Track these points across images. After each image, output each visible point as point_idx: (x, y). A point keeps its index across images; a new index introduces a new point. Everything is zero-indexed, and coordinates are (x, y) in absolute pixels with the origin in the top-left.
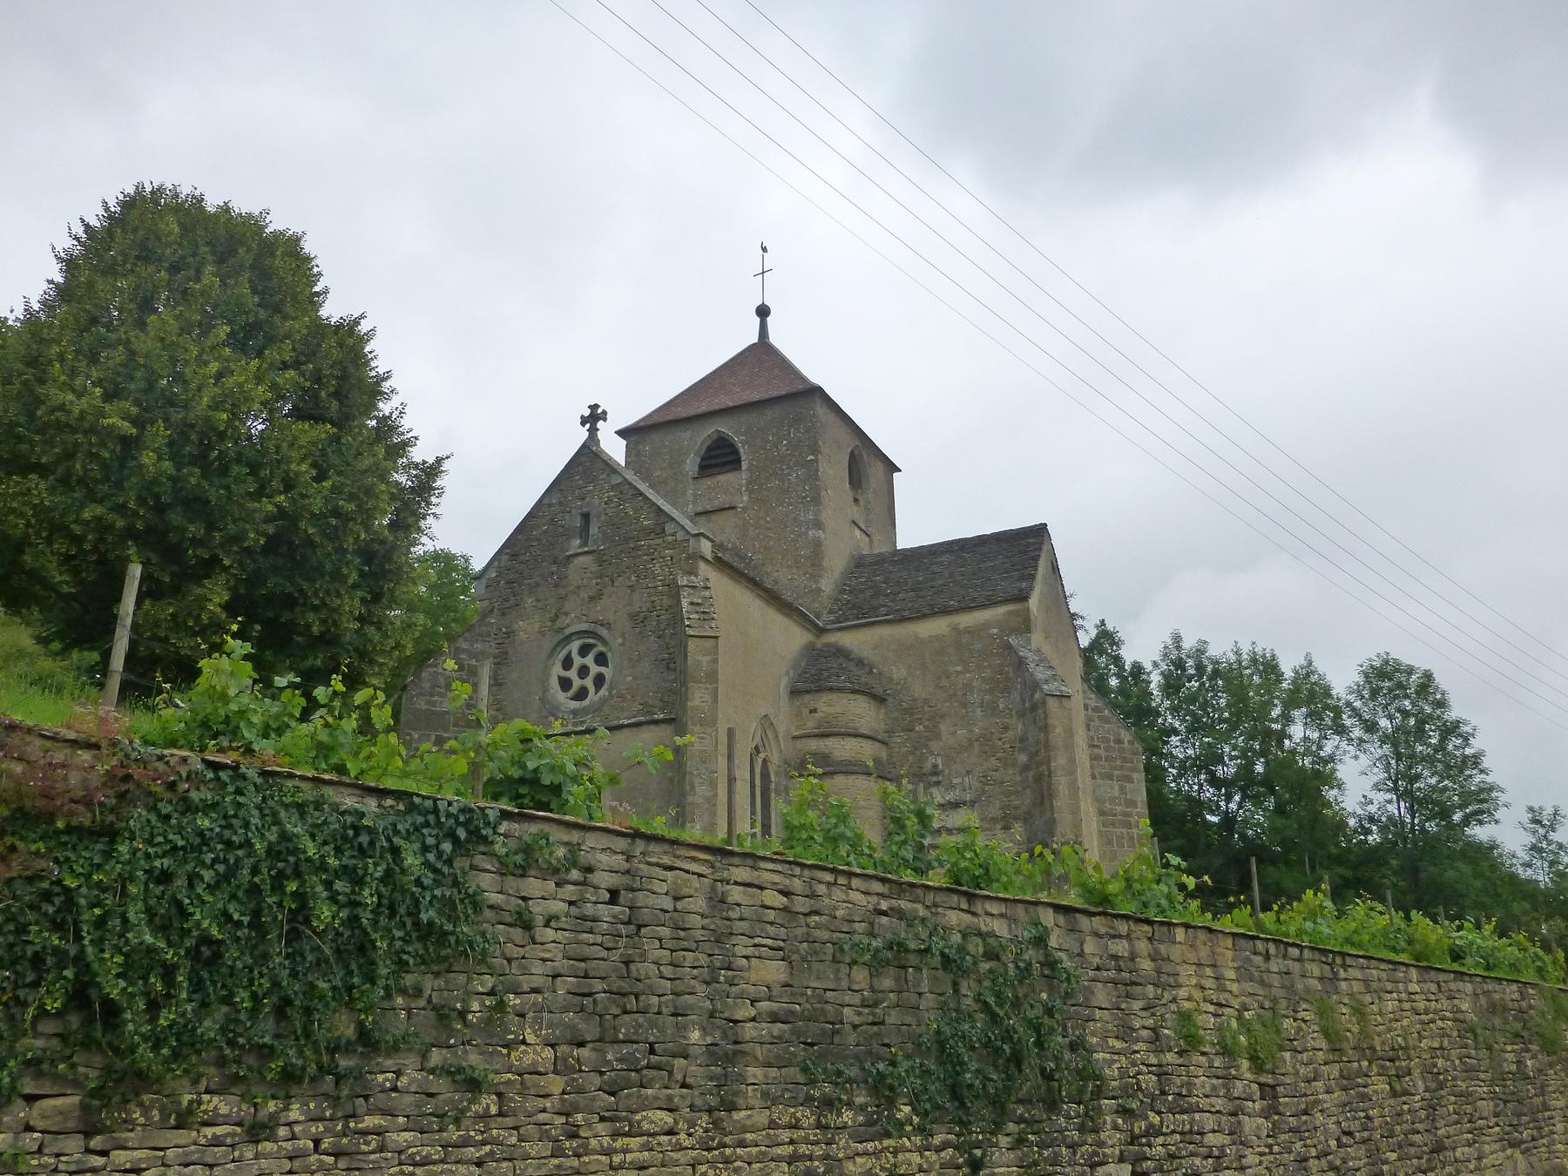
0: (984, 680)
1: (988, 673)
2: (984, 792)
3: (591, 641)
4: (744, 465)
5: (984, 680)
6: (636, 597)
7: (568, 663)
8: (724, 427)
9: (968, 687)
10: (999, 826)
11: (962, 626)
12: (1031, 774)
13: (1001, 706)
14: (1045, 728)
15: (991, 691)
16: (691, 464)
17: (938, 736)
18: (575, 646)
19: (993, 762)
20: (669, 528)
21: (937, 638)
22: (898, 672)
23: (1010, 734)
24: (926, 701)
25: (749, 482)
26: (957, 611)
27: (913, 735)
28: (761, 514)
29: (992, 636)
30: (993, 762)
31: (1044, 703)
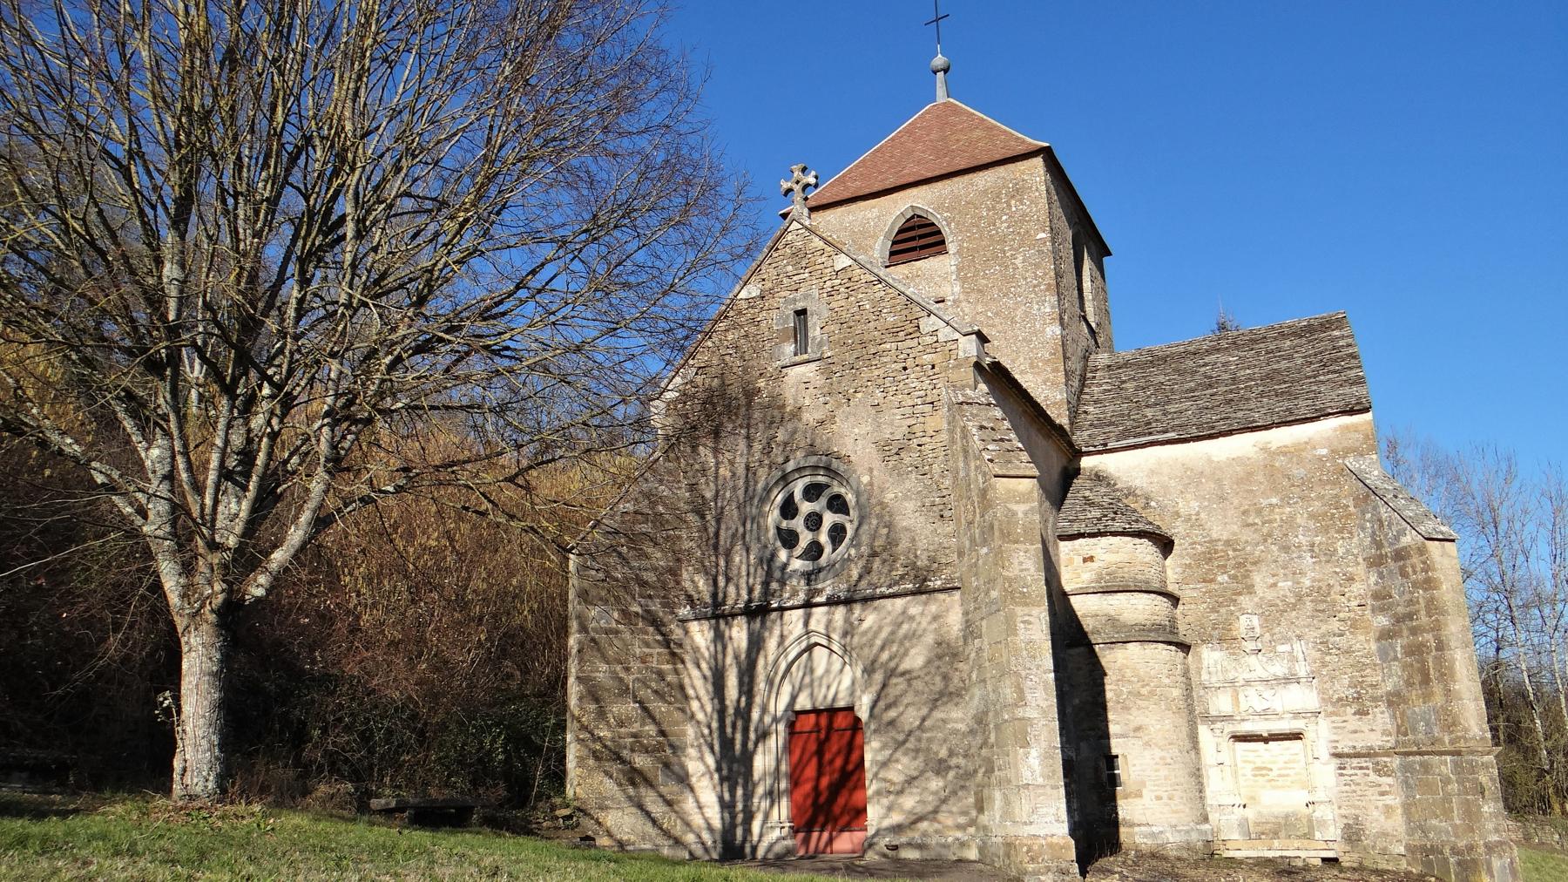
0: (1312, 516)
1: (1316, 506)
3: (821, 479)
4: (952, 247)
5: (1312, 516)
6: (885, 417)
7: (789, 509)
9: (1290, 522)
10: (1350, 710)
12: (1399, 644)
13: (1341, 551)
14: (1429, 584)
16: (879, 248)
17: (1250, 589)
18: (798, 488)
19: (1335, 625)
20: (927, 324)
21: (1239, 461)
23: (1357, 588)
24: (1228, 543)
25: (959, 270)
29: (1320, 459)
30: (1335, 625)
31: (1422, 551)
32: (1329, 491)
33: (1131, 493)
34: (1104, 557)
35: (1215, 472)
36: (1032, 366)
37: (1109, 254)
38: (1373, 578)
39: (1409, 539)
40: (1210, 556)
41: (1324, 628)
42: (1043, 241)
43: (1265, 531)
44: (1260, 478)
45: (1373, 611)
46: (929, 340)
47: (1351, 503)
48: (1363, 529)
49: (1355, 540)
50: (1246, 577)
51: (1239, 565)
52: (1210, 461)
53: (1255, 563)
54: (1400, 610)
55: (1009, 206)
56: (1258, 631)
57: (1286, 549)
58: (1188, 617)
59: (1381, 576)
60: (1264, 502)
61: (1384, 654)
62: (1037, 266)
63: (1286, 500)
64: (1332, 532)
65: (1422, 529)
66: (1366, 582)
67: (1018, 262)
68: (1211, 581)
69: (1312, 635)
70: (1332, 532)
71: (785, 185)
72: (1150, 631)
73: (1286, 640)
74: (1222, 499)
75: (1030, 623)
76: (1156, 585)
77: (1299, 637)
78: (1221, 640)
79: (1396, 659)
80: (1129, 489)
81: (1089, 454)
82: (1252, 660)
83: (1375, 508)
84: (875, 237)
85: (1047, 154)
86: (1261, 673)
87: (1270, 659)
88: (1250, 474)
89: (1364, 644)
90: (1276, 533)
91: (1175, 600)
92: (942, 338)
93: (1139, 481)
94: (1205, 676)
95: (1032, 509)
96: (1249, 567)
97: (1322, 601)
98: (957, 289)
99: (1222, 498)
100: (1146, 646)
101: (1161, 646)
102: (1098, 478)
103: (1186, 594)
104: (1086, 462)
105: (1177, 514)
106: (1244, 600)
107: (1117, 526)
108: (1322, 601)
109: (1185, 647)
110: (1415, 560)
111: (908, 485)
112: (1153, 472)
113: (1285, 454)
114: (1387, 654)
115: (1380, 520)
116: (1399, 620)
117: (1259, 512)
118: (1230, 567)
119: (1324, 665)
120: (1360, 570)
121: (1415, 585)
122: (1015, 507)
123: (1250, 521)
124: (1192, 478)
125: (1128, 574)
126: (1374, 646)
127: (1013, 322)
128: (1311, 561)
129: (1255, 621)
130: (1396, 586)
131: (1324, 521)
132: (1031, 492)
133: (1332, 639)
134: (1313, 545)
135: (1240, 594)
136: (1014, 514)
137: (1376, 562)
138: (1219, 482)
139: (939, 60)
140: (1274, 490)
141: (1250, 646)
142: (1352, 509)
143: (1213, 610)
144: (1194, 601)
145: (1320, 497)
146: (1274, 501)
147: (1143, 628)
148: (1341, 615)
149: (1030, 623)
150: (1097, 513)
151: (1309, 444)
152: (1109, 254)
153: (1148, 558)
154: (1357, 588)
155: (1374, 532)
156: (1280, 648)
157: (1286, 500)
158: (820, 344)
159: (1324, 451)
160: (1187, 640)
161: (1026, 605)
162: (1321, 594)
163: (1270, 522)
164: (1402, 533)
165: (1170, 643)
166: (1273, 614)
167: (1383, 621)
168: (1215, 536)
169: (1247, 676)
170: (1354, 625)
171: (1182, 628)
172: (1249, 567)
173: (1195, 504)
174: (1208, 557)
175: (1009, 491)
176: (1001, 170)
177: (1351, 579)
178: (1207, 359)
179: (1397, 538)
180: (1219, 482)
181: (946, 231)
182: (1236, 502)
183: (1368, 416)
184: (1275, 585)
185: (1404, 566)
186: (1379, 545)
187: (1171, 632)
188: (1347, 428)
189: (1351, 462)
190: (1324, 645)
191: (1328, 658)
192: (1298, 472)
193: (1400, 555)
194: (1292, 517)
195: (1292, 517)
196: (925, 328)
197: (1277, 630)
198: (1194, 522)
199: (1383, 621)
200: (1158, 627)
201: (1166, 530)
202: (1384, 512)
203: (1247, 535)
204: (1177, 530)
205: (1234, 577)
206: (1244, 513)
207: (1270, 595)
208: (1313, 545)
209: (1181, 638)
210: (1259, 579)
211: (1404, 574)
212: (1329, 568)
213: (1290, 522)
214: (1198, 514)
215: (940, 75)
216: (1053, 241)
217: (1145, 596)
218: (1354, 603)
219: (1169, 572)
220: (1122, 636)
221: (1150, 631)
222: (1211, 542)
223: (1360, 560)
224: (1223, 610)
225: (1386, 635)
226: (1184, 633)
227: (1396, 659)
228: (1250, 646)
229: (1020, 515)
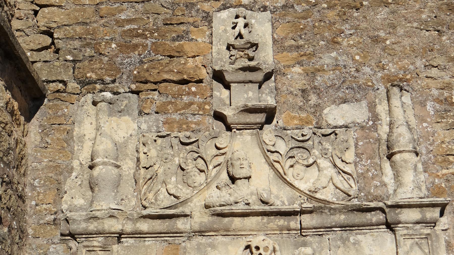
73: (352, 89)
77: (398, 84)
78: (143, 84)
82: (242, 146)
86: (260, 183)
87: (302, 145)
94: (75, 199)
129: (262, 29)
156: (335, 115)
169: (214, 196)
197: (327, 59)
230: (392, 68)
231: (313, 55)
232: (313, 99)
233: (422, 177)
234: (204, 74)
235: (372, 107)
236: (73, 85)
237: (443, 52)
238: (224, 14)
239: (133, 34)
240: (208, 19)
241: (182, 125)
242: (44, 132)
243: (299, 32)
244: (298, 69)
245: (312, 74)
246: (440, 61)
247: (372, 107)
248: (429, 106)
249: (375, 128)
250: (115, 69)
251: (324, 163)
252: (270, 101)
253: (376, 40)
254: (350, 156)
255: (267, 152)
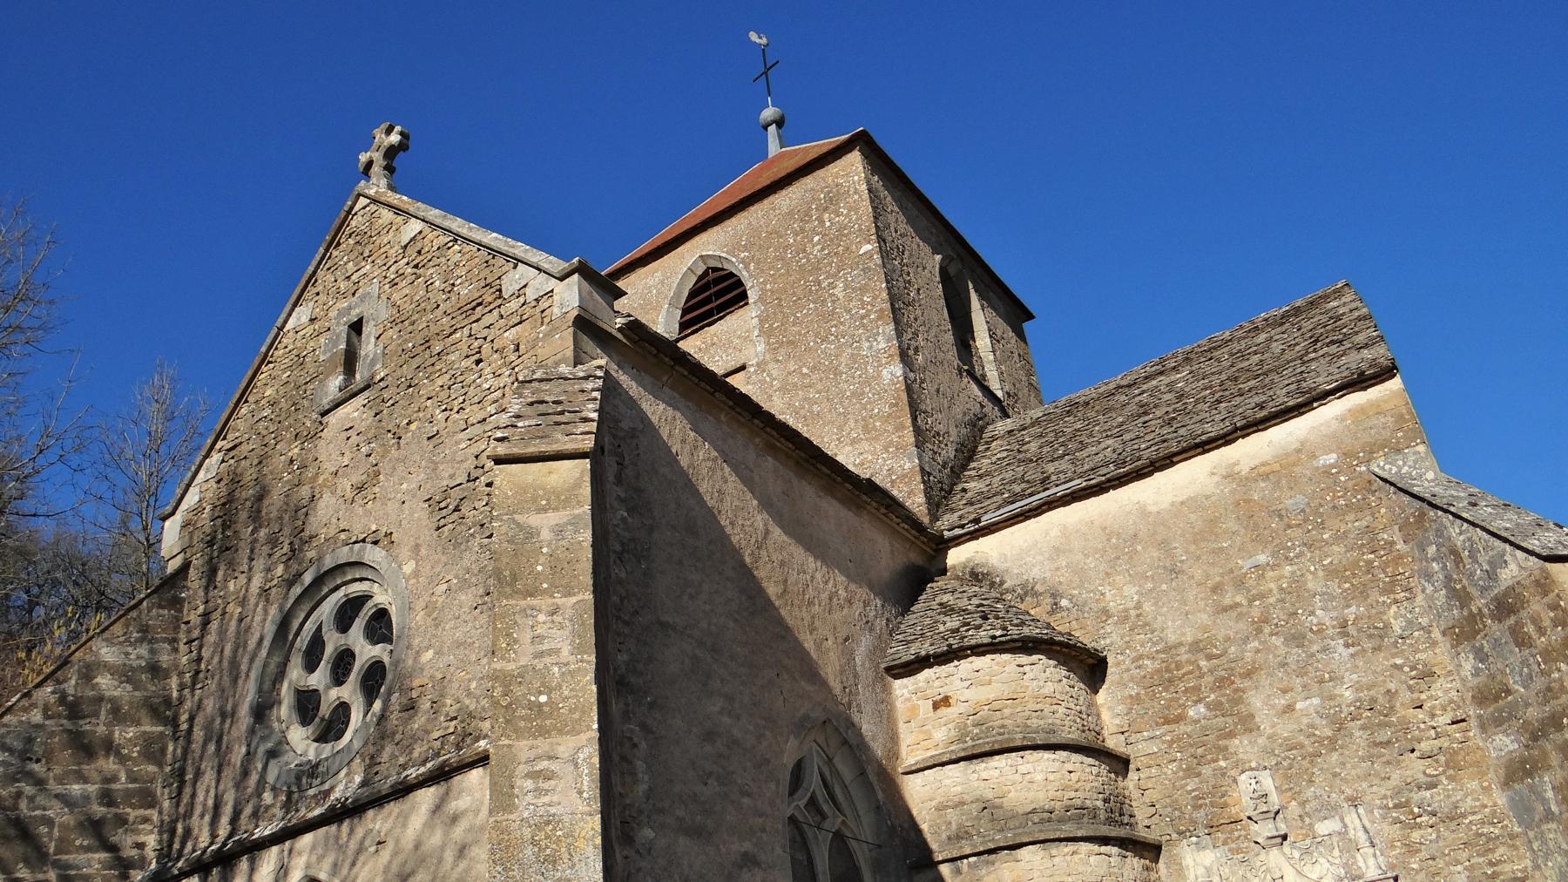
0: (1332, 573)
2: (1411, 849)
4: (752, 295)
5: (1332, 573)
8: (710, 245)
9: (1296, 590)
11: (1244, 469)
12: (1547, 783)
13: (1397, 626)
15: (1362, 593)
17: (1248, 724)
19: (1415, 768)
21: (1192, 503)
22: (1121, 594)
23: (1442, 690)
24: (1196, 647)
26: (1226, 439)
27: (1183, 728)
28: (792, 366)
29: (1326, 472)
30: (1415, 768)
31: (1544, 585)
32: (1355, 524)
33: (1028, 591)
34: (967, 694)
35: (1154, 530)
36: (866, 429)
37: (1030, 317)
38: (1468, 664)
39: (1514, 568)
40: (1167, 677)
41: (1396, 777)
42: (869, 254)
43: (1256, 614)
44: (1232, 525)
45: (1483, 727)
46: (514, 305)
47: (1397, 537)
48: (1428, 576)
49: (1420, 599)
50: (1237, 701)
51: (1221, 683)
52: (1143, 512)
53: (1248, 675)
54: (1533, 713)
55: (822, 222)
56: (1275, 800)
57: (1297, 639)
58: (1147, 791)
59: (1480, 655)
60: (1246, 564)
61: (1522, 810)
62: (863, 290)
63: (1282, 555)
64: (1375, 596)
65: (1532, 544)
66: (1455, 674)
67: (839, 291)
68: (1179, 719)
69: (1377, 792)
70: (1375, 596)
71: (363, 158)
72: (1061, 821)
73: (1330, 810)
74: (1174, 571)
75: (548, 776)
76: (1073, 736)
77: (1354, 802)
79: (1549, 816)
80: (1023, 586)
81: (957, 541)
82: (1274, 857)
83: (1439, 533)
84: (658, 308)
85: (863, 142)
88: (1213, 522)
89: (1480, 795)
90: (1277, 615)
91: (1119, 764)
92: (531, 294)
93: (1038, 571)
95: (574, 522)
96: (1239, 683)
97: (1381, 726)
98: (761, 348)
99: (1174, 571)
100: (1055, 849)
101: (1085, 847)
102: (976, 576)
103: (1139, 750)
104: (956, 557)
105: (1106, 612)
106: (1242, 746)
107: (983, 636)
108: (1381, 726)
109: (1150, 850)
110: (1536, 606)
111: (468, 559)
112: (1057, 551)
113: (1266, 477)
114: (1529, 810)
115: (1454, 552)
116: (1535, 735)
117: (1240, 583)
118: (1207, 688)
119: (1411, 849)
120: (1441, 654)
121: (1547, 655)
122: (534, 520)
123: (1228, 601)
124: (1119, 547)
125: (1011, 721)
126: (1500, 799)
127: (837, 373)
128: (1346, 652)
129: (1268, 782)
130: (1513, 668)
131: (1355, 581)
132: (577, 485)
133: (1416, 796)
134: (1344, 625)
135: (1231, 735)
136: (531, 533)
137: (1465, 633)
138: (1164, 545)
139: (769, 113)
140: (1260, 540)
141: (1264, 830)
142: (1400, 546)
143: (1190, 772)
144: (1155, 760)
145: (1339, 538)
146: (1262, 558)
147: (1048, 816)
148: (1425, 746)
149: (548, 776)
150: (953, 622)
151: (1304, 451)
152: (1030, 317)
153: (1049, 688)
154: (1442, 690)
155: (1448, 578)
156: (1323, 828)
157: (1282, 555)
158: (373, 362)
159: (1332, 458)
160: (1151, 836)
161: (543, 732)
162: (1376, 710)
163: (1261, 596)
164: (1499, 562)
165: (1104, 841)
166: (1296, 762)
167: (1505, 744)
168: (1172, 638)
170: (1454, 764)
171: (1141, 815)
172: (1239, 683)
173: (1131, 591)
174: (1167, 677)
175: (522, 489)
176: (808, 182)
177: (1427, 675)
178: (1145, 387)
179: (1491, 575)
180: (1164, 545)
181: (744, 276)
182: (1199, 574)
183: (1395, 384)
184: (1290, 708)
185: (1519, 625)
186: (1463, 598)
187: (1110, 821)
188: (1361, 411)
189: (1382, 466)
190: (1403, 810)
191: (1416, 836)
192: (1293, 501)
193: (1506, 606)
194: (1298, 581)
195: (1298, 581)
196: (510, 285)
198: (1135, 621)
199: (1505, 744)
200: (1083, 812)
201: (1085, 638)
202: (1457, 534)
203: (1228, 627)
204: (1107, 639)
205: (1215, 707)
206: (1214, 590)
207: (1285, 729)
208: (1344, 625)
209: (1142, 833)
210: (1259, 701)
211: (1522, 641)
212: (1382, 661)
213: (1296, 590)
214: (1138, 606)
215: (772, 129)
216: (885, 254)
217: (1047, 755)
218: (1443, 720)
219: (1106, 716)
220: (1010, 837)
221: (1061, 821)
222: (1168, 649)
223: (1436, 634)
224: (1206, 770)
225: (1519, 771)
226: (1145, 824)
227: (1549, 816)
228: (1264, 830)
229: (546, 535)
230: (1349, 792)
231: (1299, 793)
232: (1307, 820)
233: (1381, 859)
234: (1243, 816)
235: (1342, 820)
236: (1174, 836)
237: (1377, 775)
238: (1243, 777)
239: (1197, 798)
240: (1235, 781)
241: (1238, 851)
242: (1168, 867)
243: (1287, 778)
244: (1294, 803)
245: (1303, 804)
246: (1376, 781)
247: (1342, 820)
248: (1376, 812)
249: (1346, 832)
250: (1194, 822)
251: (1322, 860)
252: (1283, 829)
253: (1335, 775)
254: (1336, 852)
255: (1289, 859)
